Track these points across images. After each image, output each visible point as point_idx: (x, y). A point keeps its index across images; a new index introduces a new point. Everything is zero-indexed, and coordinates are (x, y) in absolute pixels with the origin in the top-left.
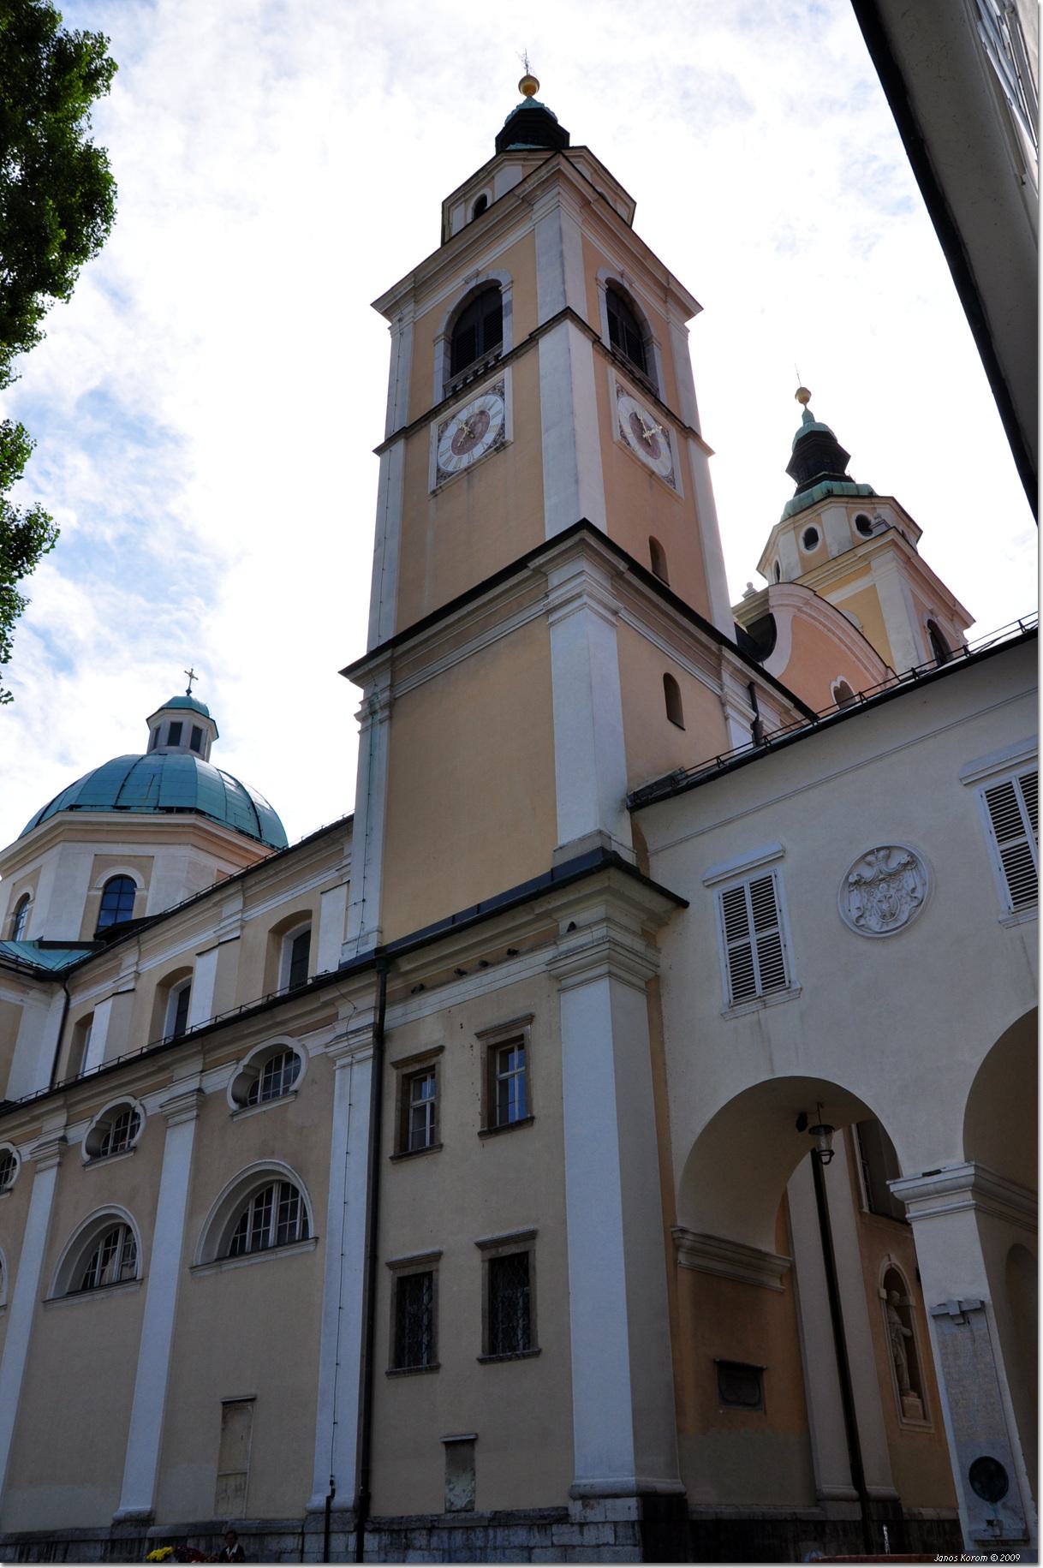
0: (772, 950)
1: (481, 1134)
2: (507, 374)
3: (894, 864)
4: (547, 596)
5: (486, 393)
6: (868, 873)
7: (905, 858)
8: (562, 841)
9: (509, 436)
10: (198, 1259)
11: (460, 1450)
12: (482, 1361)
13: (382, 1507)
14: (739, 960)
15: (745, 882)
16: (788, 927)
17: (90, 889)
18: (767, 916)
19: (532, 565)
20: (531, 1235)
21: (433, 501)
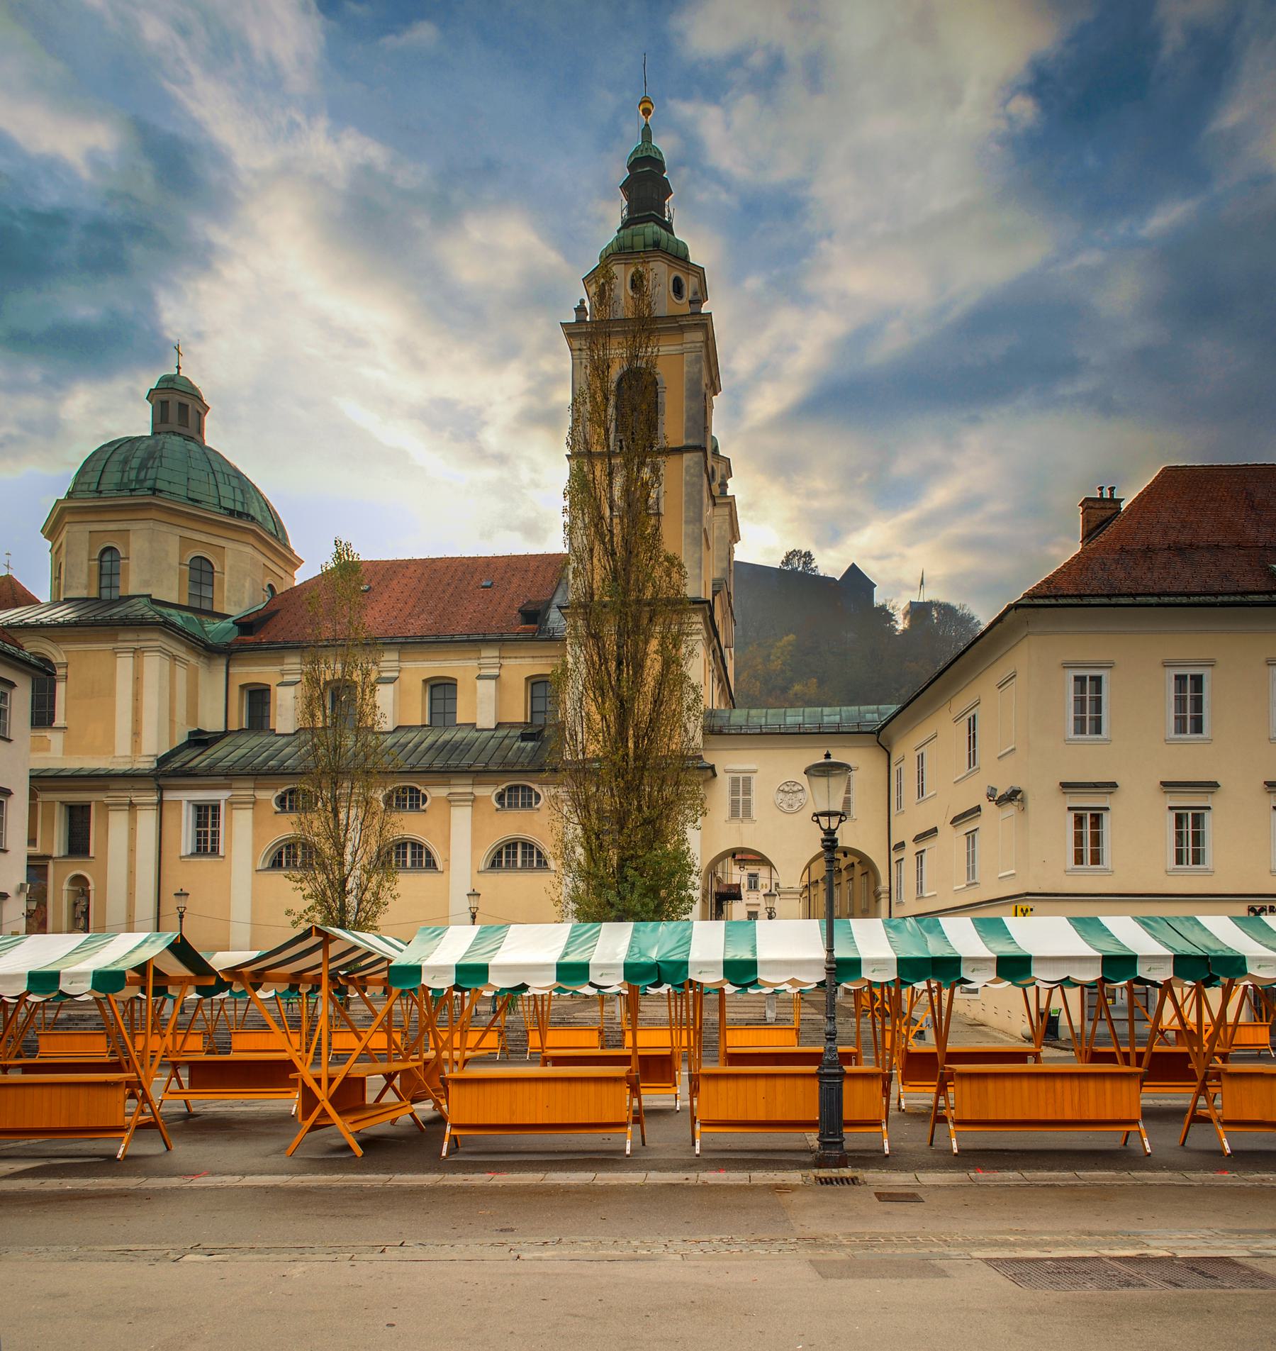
0: (747, 804)
3: (795, 789)
6: (787, 789)
7: (800, 788)
10: (482, 868)
14: (734, 803)
15: (741, 776)
16: (755, 797)
17: (180, 564)
18: (747, 791)
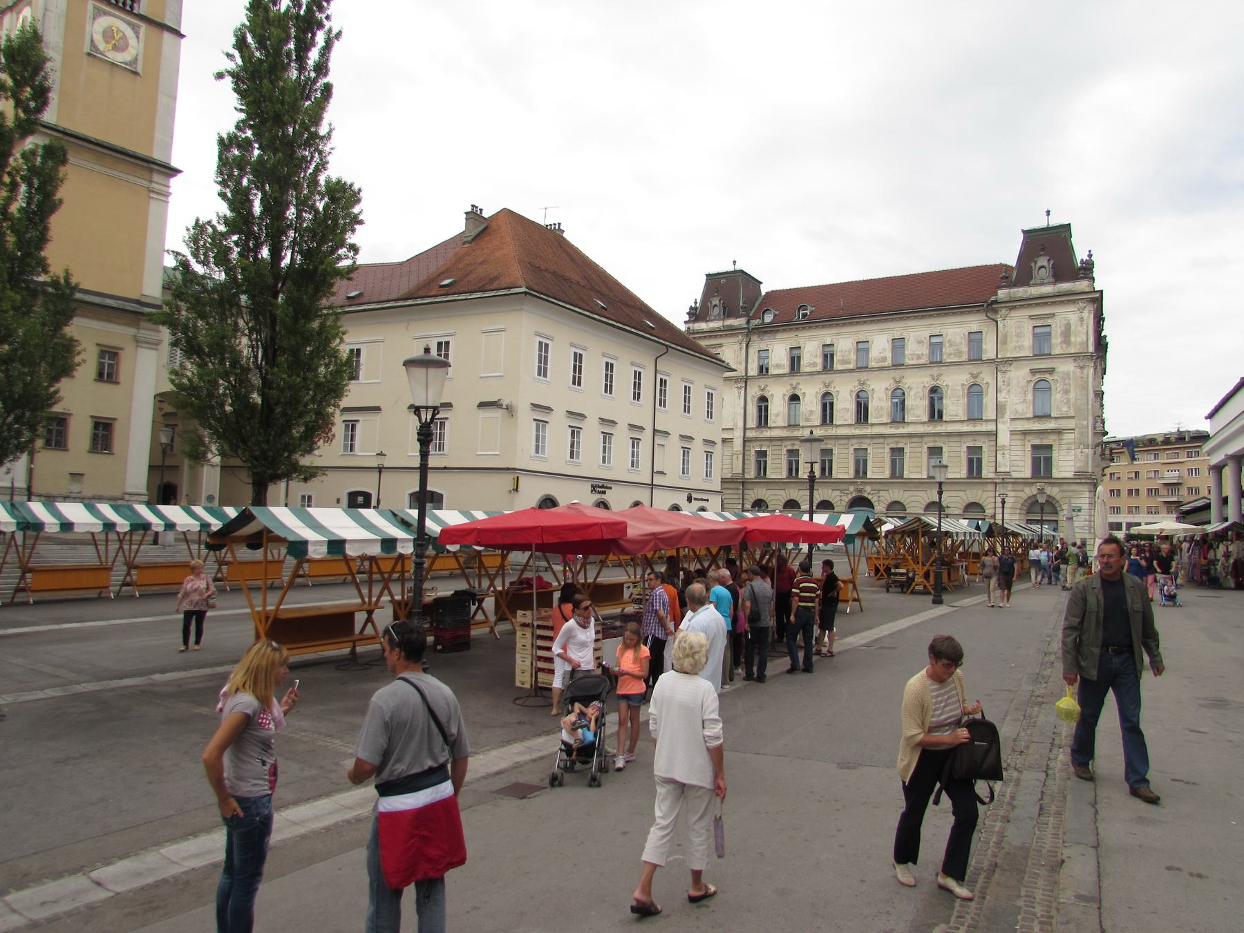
1: (95, 380)
2: (144, 27)
4: (151, 181)
5: (129, 24)
8: (145, 293)
9: (139, 70)
11: (76, 476)
12: (89, 452)
13: (34, 490)
19: (152, 166)
20: (115, 419)
21: (85, 56)
